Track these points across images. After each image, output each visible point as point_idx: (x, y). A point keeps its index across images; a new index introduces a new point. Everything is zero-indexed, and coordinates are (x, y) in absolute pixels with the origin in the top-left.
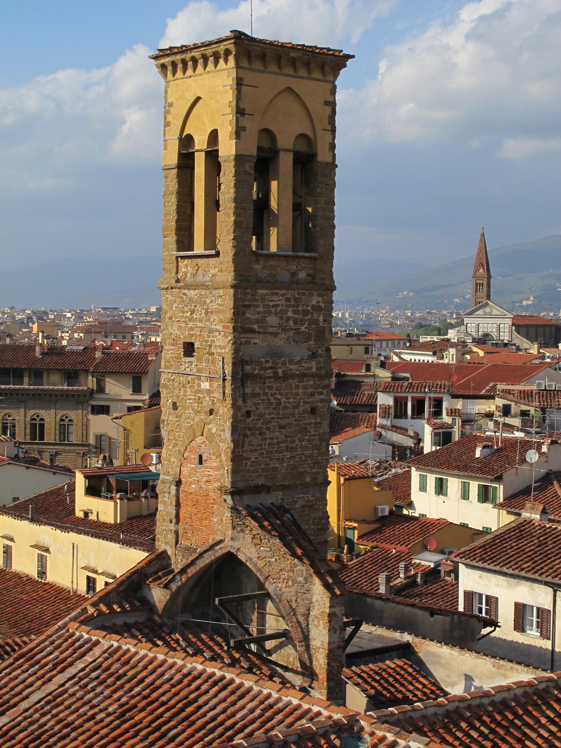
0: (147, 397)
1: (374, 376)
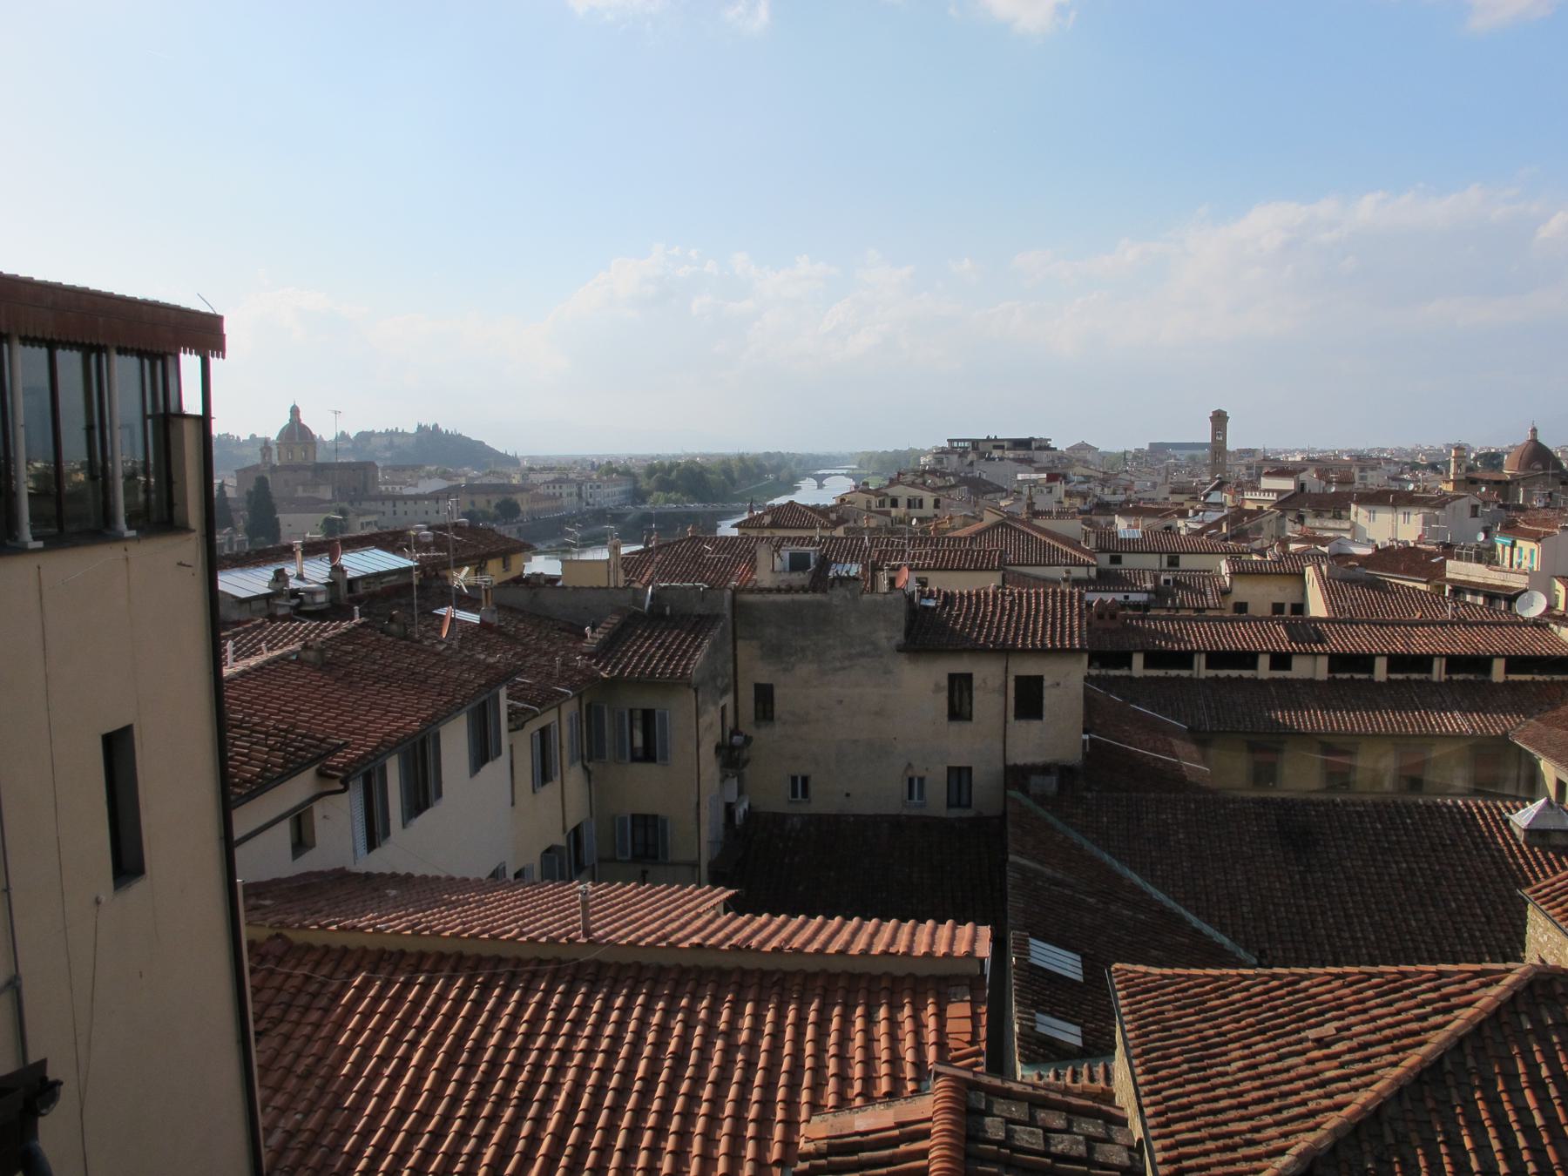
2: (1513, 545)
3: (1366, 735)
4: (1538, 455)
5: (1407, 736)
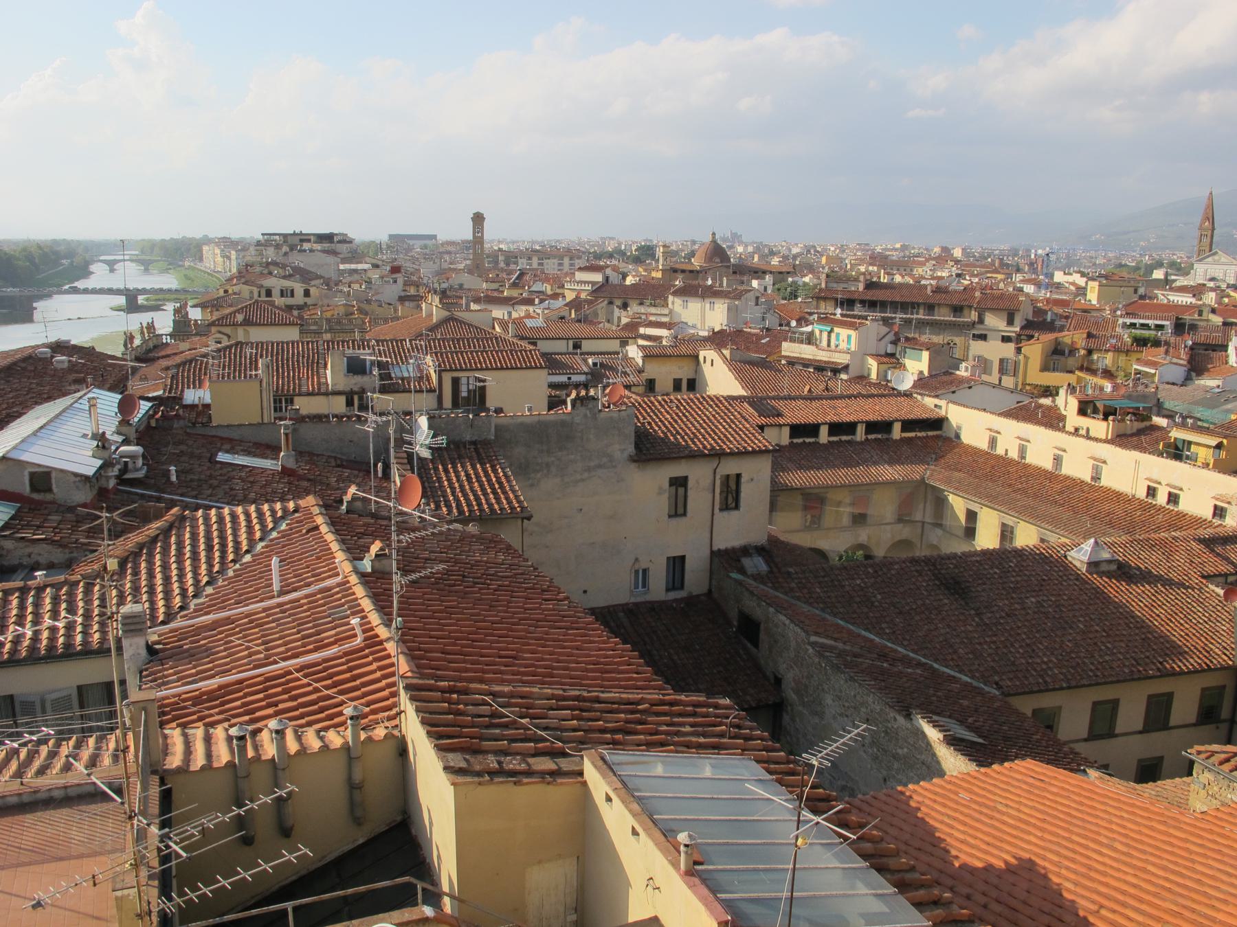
0: (1018, 329)
1: (1208, 320)
2: (830, 333)
3: (832, 487)
4: (717, 252)
5: (863, 485)
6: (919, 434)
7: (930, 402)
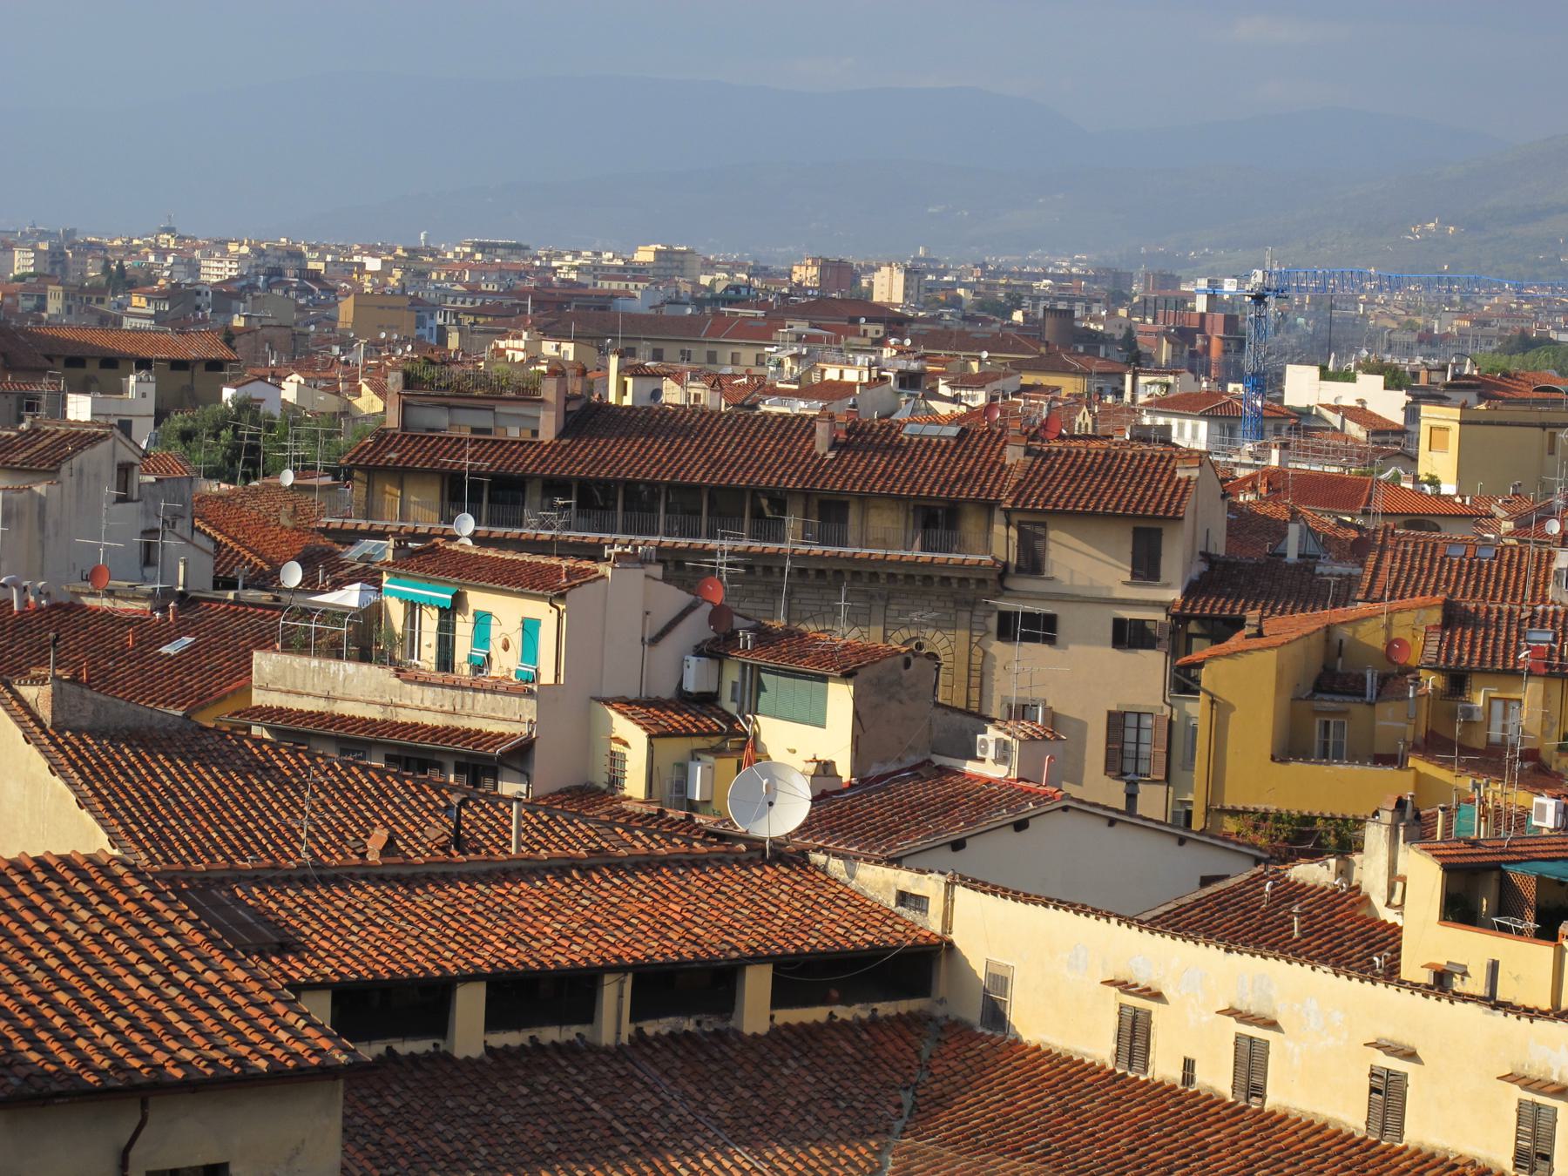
0: (1174, 595)
6: (843, 1013)
7: (878, 881)
